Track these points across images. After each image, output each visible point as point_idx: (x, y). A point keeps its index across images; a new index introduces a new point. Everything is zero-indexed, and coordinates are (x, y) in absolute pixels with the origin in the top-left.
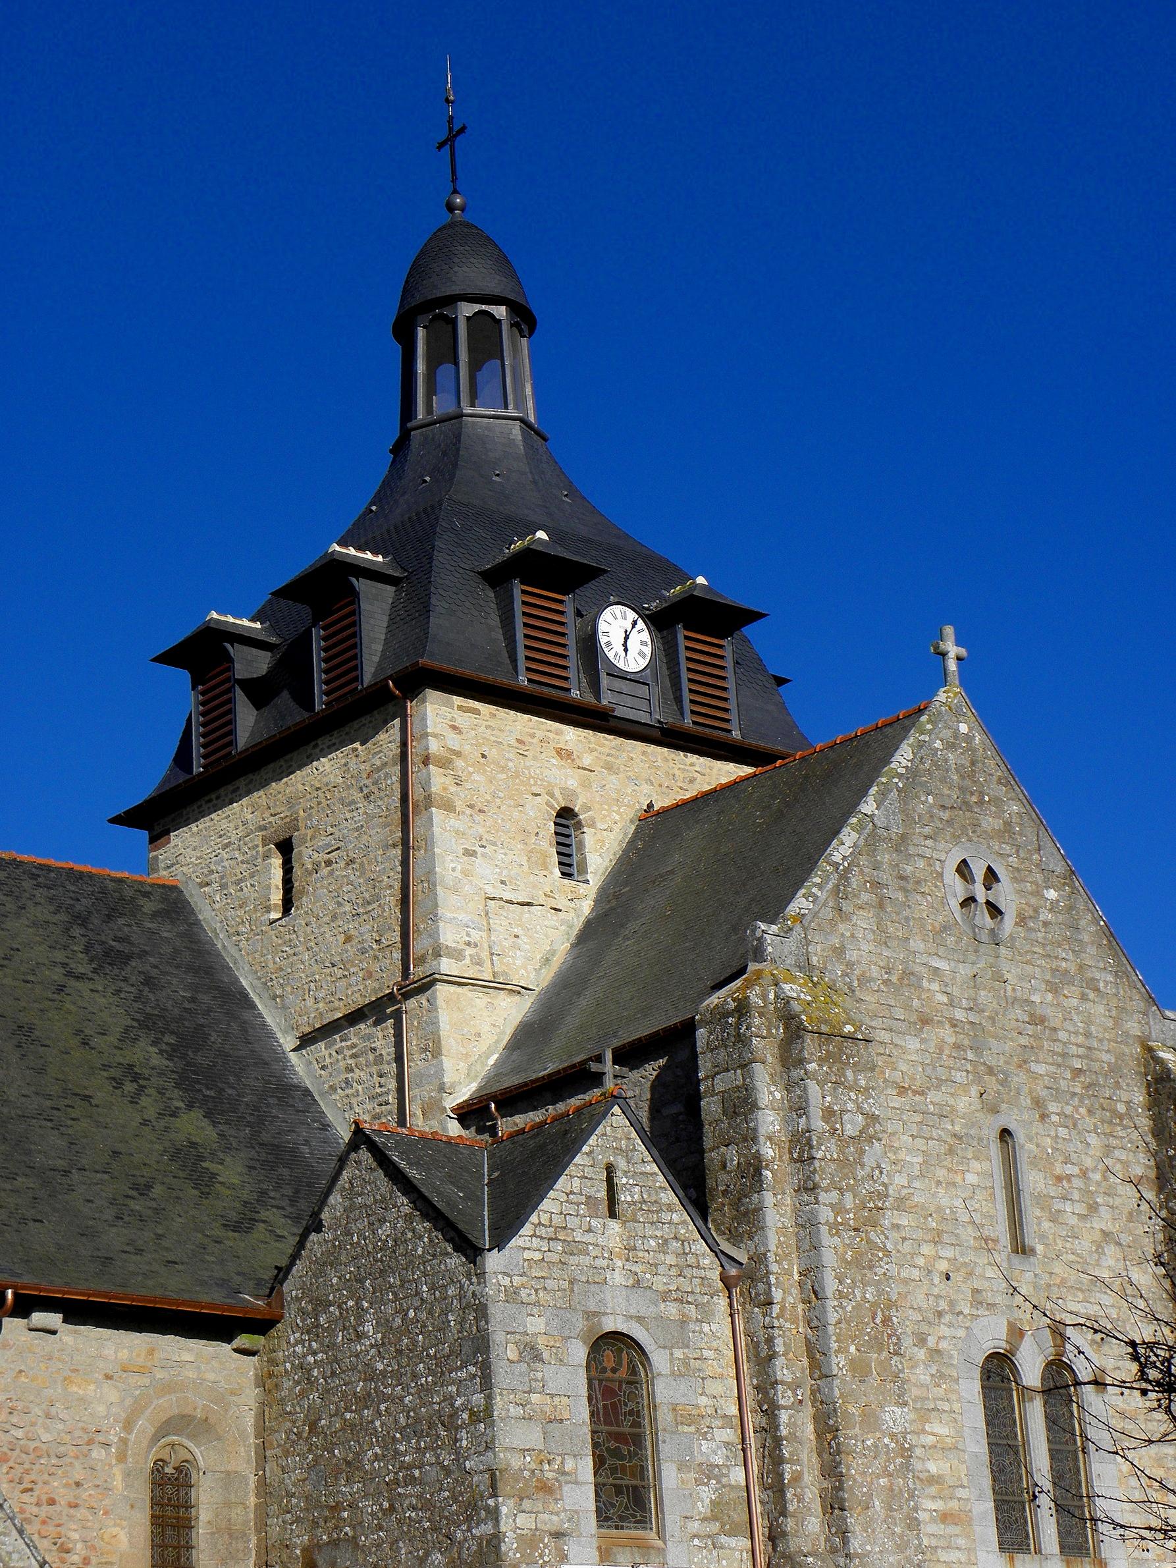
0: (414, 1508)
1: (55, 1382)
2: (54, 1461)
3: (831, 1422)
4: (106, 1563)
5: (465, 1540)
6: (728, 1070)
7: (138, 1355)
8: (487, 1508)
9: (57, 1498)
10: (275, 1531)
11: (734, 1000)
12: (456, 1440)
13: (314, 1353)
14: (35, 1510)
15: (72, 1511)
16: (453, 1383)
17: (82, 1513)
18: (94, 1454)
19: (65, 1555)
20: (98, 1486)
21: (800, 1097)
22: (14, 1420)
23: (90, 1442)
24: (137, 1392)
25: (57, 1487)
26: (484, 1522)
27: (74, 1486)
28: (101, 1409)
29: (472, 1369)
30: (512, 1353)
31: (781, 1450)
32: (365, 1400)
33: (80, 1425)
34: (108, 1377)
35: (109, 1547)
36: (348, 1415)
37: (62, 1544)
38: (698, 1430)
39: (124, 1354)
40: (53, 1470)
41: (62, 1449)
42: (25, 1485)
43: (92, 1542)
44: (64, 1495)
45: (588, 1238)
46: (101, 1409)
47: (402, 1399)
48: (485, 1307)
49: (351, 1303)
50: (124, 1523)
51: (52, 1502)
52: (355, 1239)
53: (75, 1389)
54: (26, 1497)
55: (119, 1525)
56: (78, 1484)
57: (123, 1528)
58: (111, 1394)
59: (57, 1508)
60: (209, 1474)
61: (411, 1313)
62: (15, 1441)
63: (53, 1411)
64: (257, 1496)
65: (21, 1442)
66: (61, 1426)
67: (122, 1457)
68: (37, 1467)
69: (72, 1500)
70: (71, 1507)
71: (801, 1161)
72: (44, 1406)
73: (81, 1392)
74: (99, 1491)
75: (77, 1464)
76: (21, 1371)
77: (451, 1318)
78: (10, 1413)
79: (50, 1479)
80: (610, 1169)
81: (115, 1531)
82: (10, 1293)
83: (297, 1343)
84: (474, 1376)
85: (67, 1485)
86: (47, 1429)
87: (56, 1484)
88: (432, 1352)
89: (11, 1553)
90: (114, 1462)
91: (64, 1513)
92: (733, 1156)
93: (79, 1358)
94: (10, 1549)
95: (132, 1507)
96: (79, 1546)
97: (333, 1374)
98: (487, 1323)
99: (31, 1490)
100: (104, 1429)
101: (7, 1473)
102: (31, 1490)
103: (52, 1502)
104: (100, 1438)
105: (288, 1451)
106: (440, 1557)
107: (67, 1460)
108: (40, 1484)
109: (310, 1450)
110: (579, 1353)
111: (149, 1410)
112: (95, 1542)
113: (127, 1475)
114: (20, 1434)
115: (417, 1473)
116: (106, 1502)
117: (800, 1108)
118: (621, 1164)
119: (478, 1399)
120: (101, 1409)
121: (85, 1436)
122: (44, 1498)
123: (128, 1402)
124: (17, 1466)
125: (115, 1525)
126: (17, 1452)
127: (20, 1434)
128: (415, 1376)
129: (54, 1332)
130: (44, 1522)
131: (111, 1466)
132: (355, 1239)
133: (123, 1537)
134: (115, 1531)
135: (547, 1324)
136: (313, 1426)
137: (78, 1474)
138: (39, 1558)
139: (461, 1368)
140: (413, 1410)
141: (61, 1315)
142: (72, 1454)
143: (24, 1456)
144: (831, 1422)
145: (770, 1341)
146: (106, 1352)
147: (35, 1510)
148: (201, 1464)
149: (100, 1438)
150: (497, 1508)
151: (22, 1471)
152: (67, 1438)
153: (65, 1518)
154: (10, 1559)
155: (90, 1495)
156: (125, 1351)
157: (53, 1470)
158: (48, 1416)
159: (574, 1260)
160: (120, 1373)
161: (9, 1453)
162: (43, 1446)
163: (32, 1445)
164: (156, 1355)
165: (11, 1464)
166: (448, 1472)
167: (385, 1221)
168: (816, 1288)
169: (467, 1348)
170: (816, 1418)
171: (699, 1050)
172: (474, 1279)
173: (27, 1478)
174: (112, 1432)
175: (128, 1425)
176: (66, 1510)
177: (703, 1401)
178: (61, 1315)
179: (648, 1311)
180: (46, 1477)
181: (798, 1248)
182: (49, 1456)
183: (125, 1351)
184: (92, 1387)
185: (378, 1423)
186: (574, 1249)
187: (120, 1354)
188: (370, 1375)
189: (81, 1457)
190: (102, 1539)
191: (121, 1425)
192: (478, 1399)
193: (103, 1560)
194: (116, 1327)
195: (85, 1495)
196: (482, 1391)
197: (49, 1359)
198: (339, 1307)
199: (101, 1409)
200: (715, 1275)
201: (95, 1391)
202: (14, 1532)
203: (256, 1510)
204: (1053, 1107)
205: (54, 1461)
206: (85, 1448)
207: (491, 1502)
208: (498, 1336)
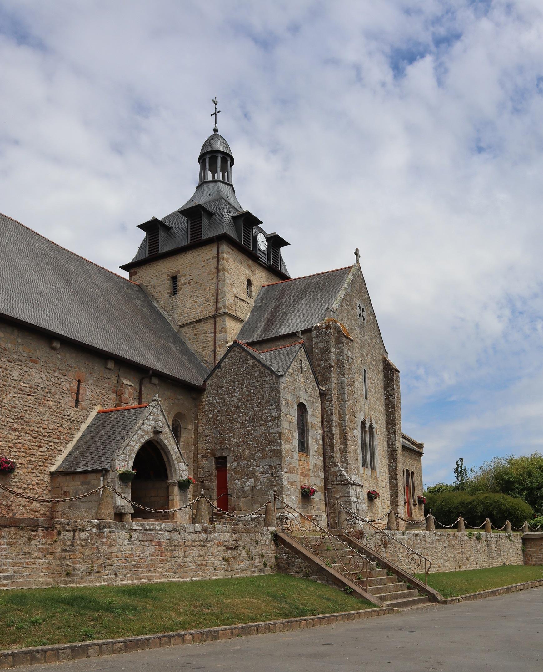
0: (251, 441)
3: (344, 431)
5: (269, 450)
6: (322, 342)
8: (277, 443)
10: (200, 446)
11: (326, 325)
12: (267, 424)
13: (217, 400)
16: (267, 410)
21: (341, 351)
26: (276, 446)
29: (274, 407)
30: (284, 404)
31: (333, 437)
32: (234, 413)
36: (228, 416)
38: (315, 430)
45: (297, 377)
47: (248, 413)
48: (279, 391)
49: (230, 387)
52: (232, 371)
60: (183, 429)
61: (252, 391)
64: (194, 436)
71: (340, 367)
76: (148, 394)
77: (266, 393)
80: (301, 361)
82: (151, 372)
83: (210, 397)
84: (274, 408)
88: (259, 401)
92: (323, 364)
97: (223, 405)
98: (280, 395)
105: (206, 425)
106: (260, 454)
109: (214, 425)
110: (296, 406)
115: (252, 432)
117: (341, 354)
118: (303, 361)
119: (275, 414)
128: (252, 407)
132: (232, 371)
135: (290, 397)
136: (215, 419)
139: (269, 406)
140: (252, 416)
144: (344, 431)
145: (331, 410)
148: (181, 426)
150: (281, 442)
159: (295, 382)
166: (263, 432)
167: (243, 367)
168: (343, 398)
169: (272, 401)
170: (339, 430)
171: (313, 337)
172: (275, 383)
177: (316, 423)
179: (307, 398)
181: (338, 388)
185: (239, 419)
186: (295, 380)
188: (236, 406)
192: (275, 414)
196: (277, 412)
198: (226, 389)
200: (318, 392)
203: (194, 439)
204: (371, 367)
207: (279, 441)
208: (282, 399)
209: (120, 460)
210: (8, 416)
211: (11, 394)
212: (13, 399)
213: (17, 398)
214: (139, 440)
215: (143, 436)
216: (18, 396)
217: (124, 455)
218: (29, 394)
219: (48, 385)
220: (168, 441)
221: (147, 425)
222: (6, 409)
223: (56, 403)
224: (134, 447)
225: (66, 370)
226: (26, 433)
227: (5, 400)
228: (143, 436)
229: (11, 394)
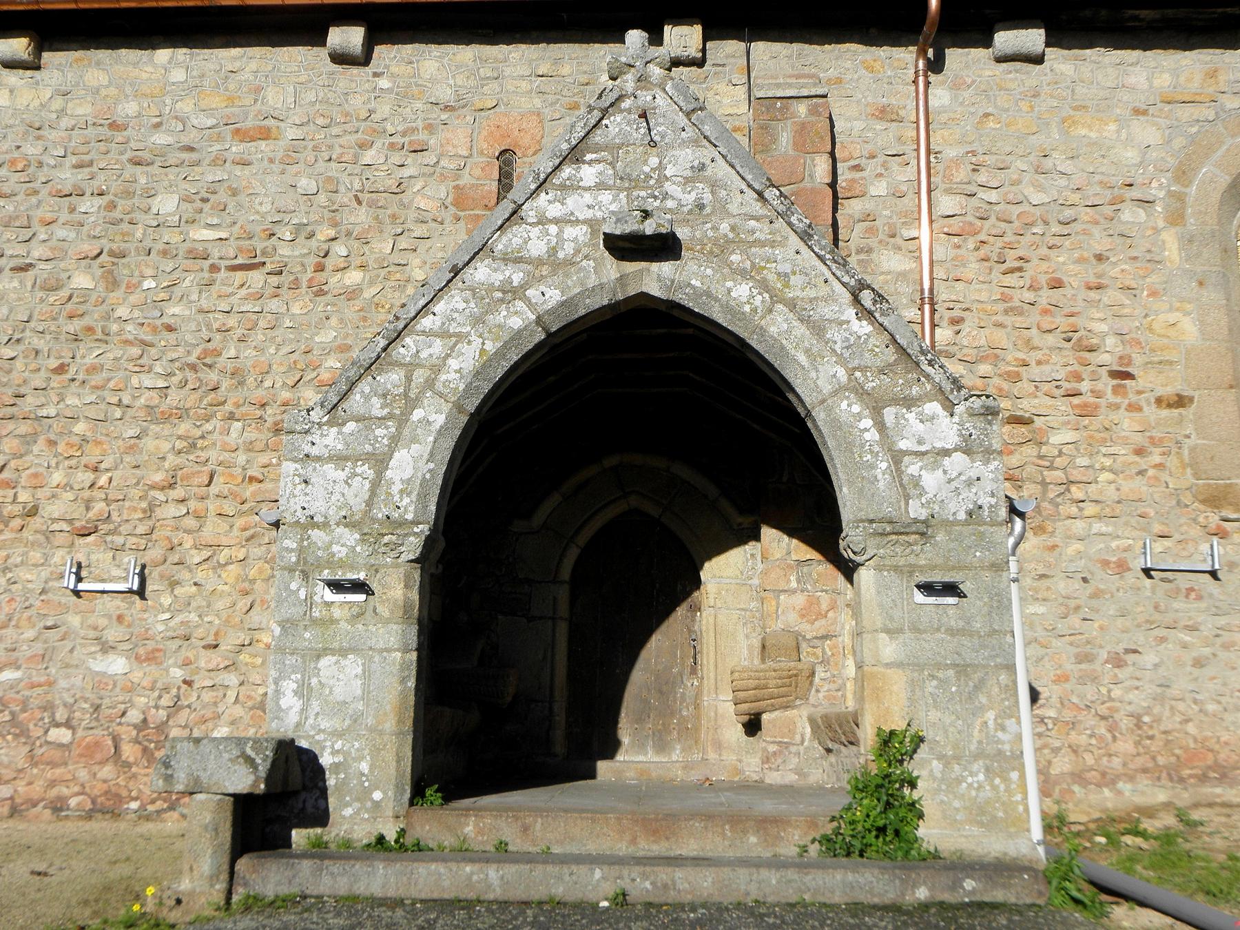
1: (1048, 124)
2: (1056, 228)
4: (1160, 363)
7: (1189, 80)
9: (1065, 279)
14: (1029, 296)
15: (1093, 295)
17: (1111, 296)
18: (1126, 216)
19: (1087, 355)
20: (1135, 258)
22: (982, 178)
23: (1117, 201)
24: (1194, 130)
25: (1064, 263)
27: (1094, 262)
28: (1131, 155)
33: (1097, 178)
34: (1137, 112)
35: (1166, 341)
37: (1080, 340)
39: (1164, 81)
40: (1057, 241)
41: (1068, 213)
42: (1011, 264)
43: (1133, 335)
44: (1075, 275)
46: (1129, 154)
50: (1189, 307)
51: (1056, 285)
53: (1083, 132)
54: (1011, 280)
55: (1178, 310)
56: (1099, 258)
57: (1187, 314)
58: (1147, 133)
59: (1068, 291)
62: (988, 207)
63: (1048, 164)
65: (997, 208)
66: (1063, 182)
67: (1176, 218)
68: (1028, 238)
69: (1093, 280)
70: (1090, 289)
72: (1031, 158)
73: (1093, 135)
74: (1138, 265)
75: (1096, 231)
76: (987, 115)
78: (974, 170)
79: (1052, 253)
81: (1172, 317)
85: (1082, 260)
86: (1040, 188)
87: (1061, 259)
89: (786, 275)
90: (1161, 224)
91: (1080, 298)
93: (1085, 91)
94: (787, 268)
95: (1201, 284)
96: (1111, 341)
99: (1020, 269)
100: (1139, 180)
101: (977, 249)
102: (1020, 269)
103: (1056, 285)
104: (1135, 193)
107: (1076, 227)
108: (1035, 261)
111: (1220, 153)
112: (1138, 335)
113: (1188, 241)
114: (993, 196)
116: (1153, 279)
120: (1129, 154)
121: (1108, 192)
122: (1043, 279)
123: (1178, 142)
124: (992, 239)
125: (1171, 309)
126: (993, 219)
127: (993, 196)
129: (1038, 60)
130: (1045, 312)
131: (1157, 231)
133: (1189, 329)
134: (1172, 317)
137: (1099, 242)
138: (846, 279)
141: (1042, 31)
142: (1086, 218)
143: (1003, 225)
146: (1132, 80)
147: (1029, 296)
149: (1135, 193)
151: (1001, 245)
152: (1075, 198)
153: (1083, 304)
154: (787, 285)
155: (1123, 271)
156: (1166, 76)
157: (1057, 241)
158: (1040, 171)
160: (1160, 105)
161: (979, 223)
162: (1033, 209)
163: (1016, 210)
164: (1222, 78)
165: (983, 237)
173: (1011, 255)
174: (1155, 184)
175: (1183, 174)
176: (1084, 293)
178: (1042, 31)
180: (1044, 251)
182: (1046, 223)
183: (1166, 76)
184: (1112, 127)
187: (1156, 83)
189: (1102, 220)
190: (1150, 329)
191: (1169, 175)
193: (1156, 359)
194: (1146, 46)
195: (1114, 272)
197: (1034, 96)
199: (1131, 155)
201: (1118, 131)
202: (794, 241)
205: (1056, 228)
206: (1108, 210)
209: (318, 459)
210: (137, 369)
211: (148, 283)
212: (162, 296)
213: (178, 292)
214: (478, 320)
215: (512, 293)
216: (187, 283)
217: (351, 426)
218: (239, 261)
219: (334, 208)
220: (764, 286)
221: (556, 221)
222: (127, 342)
223: (383, 272)
224: (437, 368)
225: (430, 128)
226: (231, 417)
227: (122, 312)
228: (512, 293)
229: (148, 283)
